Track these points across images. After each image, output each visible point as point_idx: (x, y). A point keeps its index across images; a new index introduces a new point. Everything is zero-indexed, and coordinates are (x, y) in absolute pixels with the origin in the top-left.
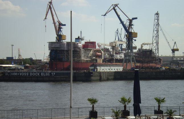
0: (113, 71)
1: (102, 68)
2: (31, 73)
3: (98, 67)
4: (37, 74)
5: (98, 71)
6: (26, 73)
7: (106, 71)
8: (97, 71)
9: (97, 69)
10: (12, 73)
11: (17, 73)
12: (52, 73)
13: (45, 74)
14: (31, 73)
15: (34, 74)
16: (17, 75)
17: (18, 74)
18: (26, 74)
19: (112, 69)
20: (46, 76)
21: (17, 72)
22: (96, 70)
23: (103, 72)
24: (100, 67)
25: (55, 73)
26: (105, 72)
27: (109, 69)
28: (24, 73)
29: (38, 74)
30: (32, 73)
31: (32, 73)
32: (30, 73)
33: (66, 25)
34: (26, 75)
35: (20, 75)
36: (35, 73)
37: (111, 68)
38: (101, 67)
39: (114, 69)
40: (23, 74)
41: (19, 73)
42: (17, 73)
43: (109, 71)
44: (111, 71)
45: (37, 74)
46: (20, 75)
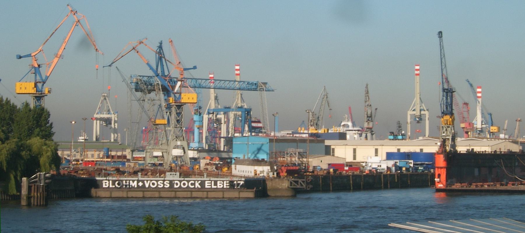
4: (192, 184)
6: (164, 181)
11: (138, 181)
12: (235, 182)
13: (216, 184)
14: (176, 182)
15: (184, 184)
16: (138, 186)
17: (141, 184)
18: (164, 185)
20: (217, 190)
28: (157, 181)
29: (197, 185)
30: (180, 181)
31: (180, 181)
33: (197, 67)
34: (163, 187)
35: (147, 186)
40: (153, 184)
45: (192, 184)
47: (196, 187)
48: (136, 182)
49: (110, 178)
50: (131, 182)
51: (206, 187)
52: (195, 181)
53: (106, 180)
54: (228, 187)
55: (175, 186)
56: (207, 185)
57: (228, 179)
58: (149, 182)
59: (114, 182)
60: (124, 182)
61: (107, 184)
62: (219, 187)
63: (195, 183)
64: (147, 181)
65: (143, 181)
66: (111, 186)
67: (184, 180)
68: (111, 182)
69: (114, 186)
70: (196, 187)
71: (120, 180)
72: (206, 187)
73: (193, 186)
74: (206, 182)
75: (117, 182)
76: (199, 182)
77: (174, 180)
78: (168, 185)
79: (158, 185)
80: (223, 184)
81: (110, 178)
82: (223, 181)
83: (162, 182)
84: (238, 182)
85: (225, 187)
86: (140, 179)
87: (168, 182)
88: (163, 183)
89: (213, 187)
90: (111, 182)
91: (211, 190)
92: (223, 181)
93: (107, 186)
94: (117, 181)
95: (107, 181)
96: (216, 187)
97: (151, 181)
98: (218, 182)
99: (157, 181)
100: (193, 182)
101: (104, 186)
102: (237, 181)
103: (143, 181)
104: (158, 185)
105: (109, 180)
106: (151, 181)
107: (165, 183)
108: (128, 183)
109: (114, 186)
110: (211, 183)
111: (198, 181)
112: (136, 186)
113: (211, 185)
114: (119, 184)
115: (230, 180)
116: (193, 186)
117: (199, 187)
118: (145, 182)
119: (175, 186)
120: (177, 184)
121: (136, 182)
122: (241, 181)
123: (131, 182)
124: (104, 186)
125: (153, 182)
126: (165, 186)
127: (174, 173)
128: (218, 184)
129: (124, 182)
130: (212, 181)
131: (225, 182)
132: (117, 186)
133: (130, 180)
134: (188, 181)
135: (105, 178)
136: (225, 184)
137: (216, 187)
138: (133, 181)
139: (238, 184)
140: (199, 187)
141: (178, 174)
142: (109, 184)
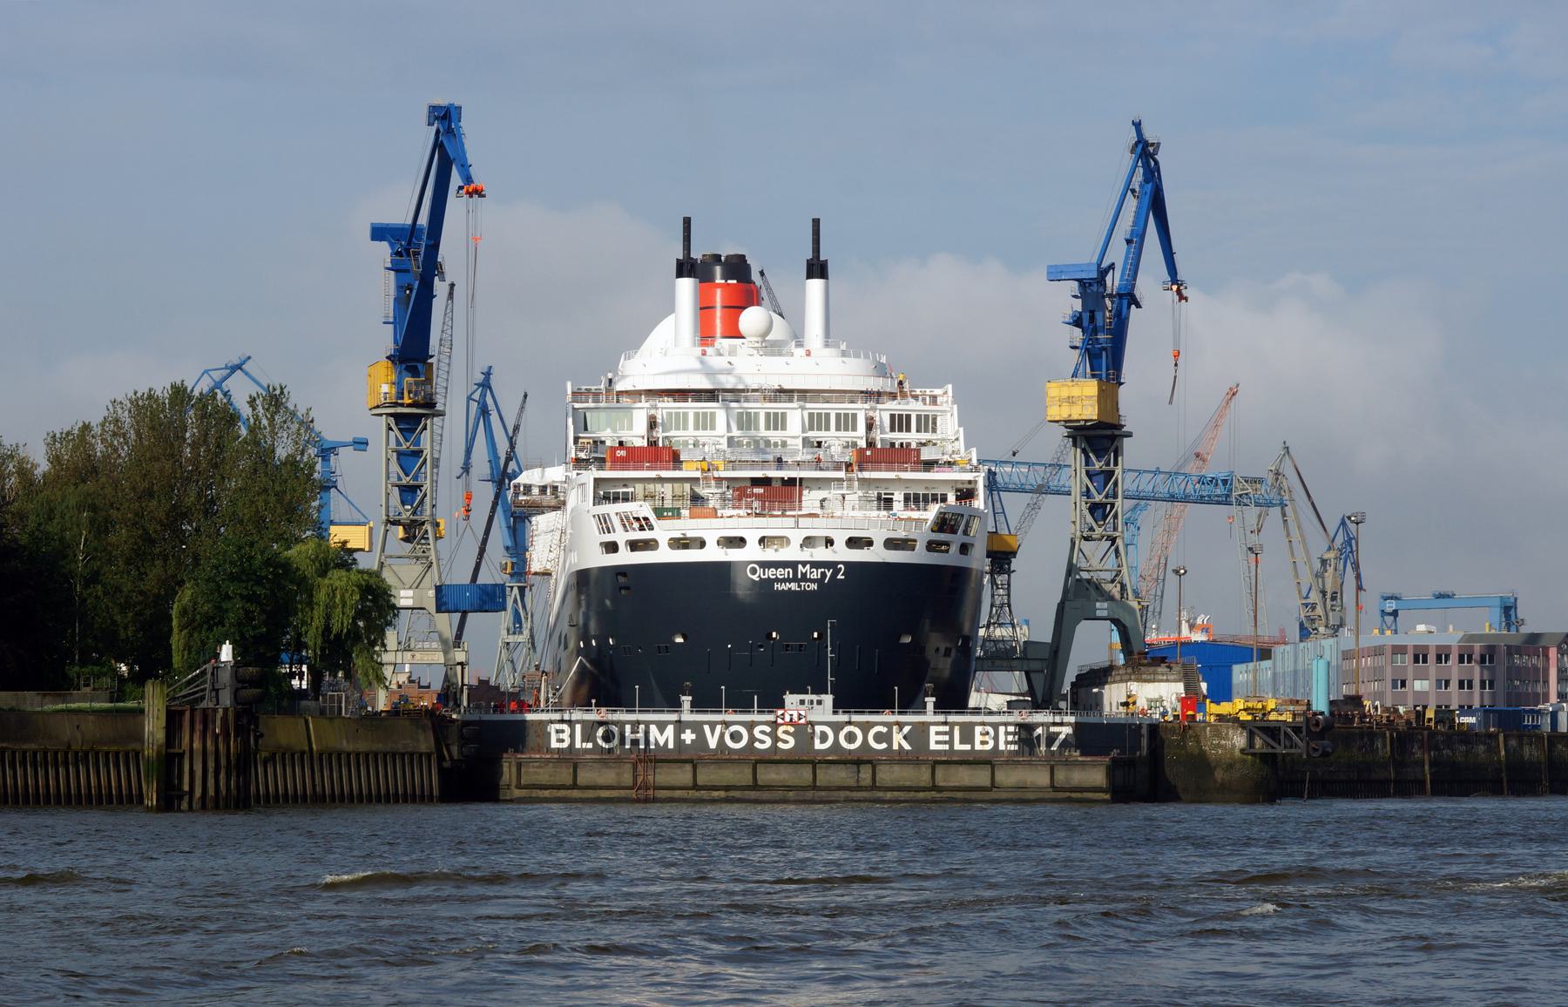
2: (818, 729)
4: (879, 738)
6: (774, 725)
10: (621, 724)
11: (680, 726)
12: (1039, 731)
13: (967, 737)
14: (818, 729)
15: (851, 738)
18: (776, 739)
28: (750, 726)
29: (898, 740)
31: (837, 727)
34: (774, 746)
35: (713, 743)
40: (736, 737)
41: (697, 727)
45: (879, 738)
46: (713, 743)
47: (896, 747)
48: (670, 730)
49: (574, 717)
50: (653, 728)
51: (933, 746)
52: (889, 725)
53: (562, 721)
54: (1013, 747)
55: (818, 745)
56: (936, 741)
57: (1011, 719)
58: (719, 728)
59: (589, 730)
60: (628, 728)
61: (565, 736)
62: (978, 747)
63: (890, 733)
64: (713, 725)
65: (697, 727)
66: (578, 745)
67: (850, 723)
68: (578, 727)
69: (590, 745)
70: (896, 747)
71: (613, 723)
72: (933, 746)
73: (884, 746)
74: (933, 729)
75: (600, 732)
76: (906, 729)
77: (812, 724)
78: (792, 742)
79: (752, 739)
80: (996, 738)
81: (577, 715)
83: (768, 729)
84: (1053, 729)
86: (687, 716)
87: (791, 729)
89: (958, 746)
90: (578, 727)
91: (952, 760)
92: (995, 726)
93: (565, 745)
94: (601, 723)
95: (565, 727)
96: (968, 747)
97: (727, 724)
98: (978, 729)
99: (750, 726)
100: (884, 730)
101: (554, 744)
102: (1046, 725)
104: (752, 739)
105: (570, 723)
107: (781, 729)
108: (641, 735)
109: (590, 745)
110: (951, 734)
111: (901, 725)
112: (671, 746)
113: (951, 742)
114: (607, 737)
115: (1019, 720)
116: (884, 746)
117: (907, 747)
118: (707, 728)
119: (818, 745)
120: (824, 738)
122: (1061, 724)
123: (653, 728)
124: (554, 744)
125: (733, 728)
126: (780, 745)
127: (815, 698)
128: (978, 738)
129: (628, 728)
131: (1002, 729)
132: (600, 742)
133: (647, 724)
135: (557, 716)
137: (968, 747)
138: (662, 726)
139: (1051, 738)
140: (907, 747)
141: (828, 699)
142: (572, 736)
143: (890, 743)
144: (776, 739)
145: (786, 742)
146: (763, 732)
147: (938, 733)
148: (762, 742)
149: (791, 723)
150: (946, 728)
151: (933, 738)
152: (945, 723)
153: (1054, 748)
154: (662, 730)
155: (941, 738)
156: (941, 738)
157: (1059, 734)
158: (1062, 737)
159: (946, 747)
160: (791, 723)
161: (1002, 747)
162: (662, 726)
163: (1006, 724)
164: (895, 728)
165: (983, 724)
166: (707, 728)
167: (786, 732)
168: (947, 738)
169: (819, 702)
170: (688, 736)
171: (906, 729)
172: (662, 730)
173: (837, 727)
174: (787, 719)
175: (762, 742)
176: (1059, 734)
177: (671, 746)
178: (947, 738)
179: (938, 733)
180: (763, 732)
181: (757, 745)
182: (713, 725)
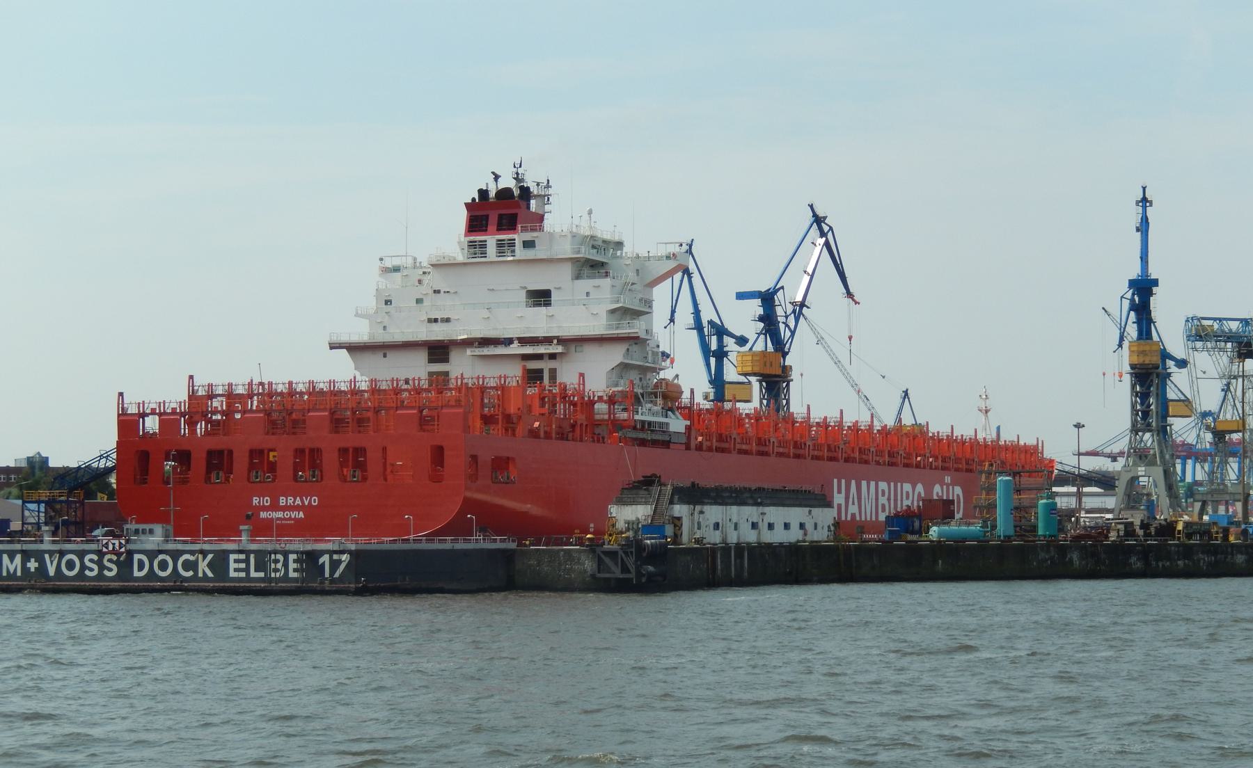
0: (778, 537)
1: (713, 513)
2: (136, 557)
3: (680, 510)
4: (188, 565)
5: (685, 538)
6: (101, 554)
7: (733, 538)
8: (677, 537)
9: (676, 522)
11: (26, 555)
12: (325, 559)
15: (163, 566)
17: (33, 565)
18: (102, 567)
19: (771, 526)
21: (23, 552)
22: (669, 530)
23: (726, 549)
24: (698, 508)
25: (350, 552)
26: (739, 548)
27: (754, 526)
28: (81, 554)
29: (203, 566)
32: (130, 553)
34: (100, 576)
35: (52, 571)
36: (175, 555)
37: (767, 519)
38: (707, 508)
39: (787, 526)
40: (70, 565)
41: (39, 556)
42: (26, 555)
43: (751, 537)
44: (769, 537)
45: (188, 565)
47: (200, 575)
48: (18, 558)
50: (5, 557)
51: (232, 574)
55: (136, 573)
56: (234, 569)
67: (161, 552)
70: (200, 575)
72: (232, 574)
73: (191, 573)
74: (232, 557)
76: (210, 556)
80: (286, 565)
82: (286, 554)
83: (95, 557)
84: (335, 557)
85: (292, 574)
87: (115, 558)
88: (99, 563)
89: (253, 574)
96: (262, 575)
99: (81, 554)
100: (192, 558)
102: (331, 553)
103: (39, 556)
106: (62, 553)
107: (108, 557)
110: (247, 561)
111: (204, 553)
112: (19, 573)
113: (247, 570)
116: (191, 573)
117: (210, 574)
118: (47, 556)
119: (136, 573)
120: (141, 567)
121: (18, 558)
123: (5, 557)
126: (106, 573)
127: (147, 527)
130: (247, 553)
131: (292, 557)
134: (175, 555)
136: (292, 566)
137: (262, 575)
138: (12, 555)
140: (210, 574)
143: (196, 571)
144: (102, 567)
145: (110, 570)
146: (91, 561)
147: (236, 561)
148: (91, 570)
149: (114, 552)
150: (242, 557)
151: (232, 566)
152: (240, 552)
153: (337, 575)
154: (12, 560)
155: (236, 566)
156: (236, 566)
157: (340, 562)
158: (342, 566)
159: (243, 575)
160: (114, 552)
161: (292, 574)
162: (12, 555)
163: (297, 552)
164: (200, 556)
165: (276, 552)
166: (47, 556)
167: (109, 560)
168: (243, 566)
169: (151, 532)
170: (33, 565)
171: (210, 556)
172: (12, 560)
173: (152, 555)
174: (111, 548)
175: (91, 570)
176: (340, 562)
177: (19, 573)
178: (243, 566)
179: (236, 561)
180: (91, 561)
181: (87, 573)
182: (51, 553)
